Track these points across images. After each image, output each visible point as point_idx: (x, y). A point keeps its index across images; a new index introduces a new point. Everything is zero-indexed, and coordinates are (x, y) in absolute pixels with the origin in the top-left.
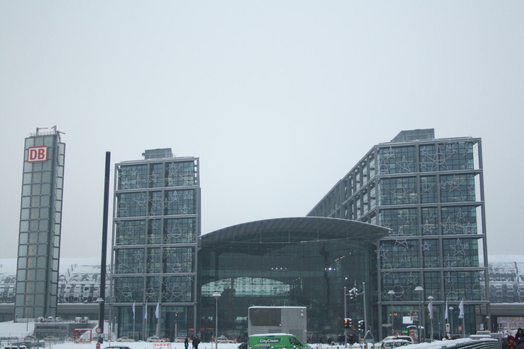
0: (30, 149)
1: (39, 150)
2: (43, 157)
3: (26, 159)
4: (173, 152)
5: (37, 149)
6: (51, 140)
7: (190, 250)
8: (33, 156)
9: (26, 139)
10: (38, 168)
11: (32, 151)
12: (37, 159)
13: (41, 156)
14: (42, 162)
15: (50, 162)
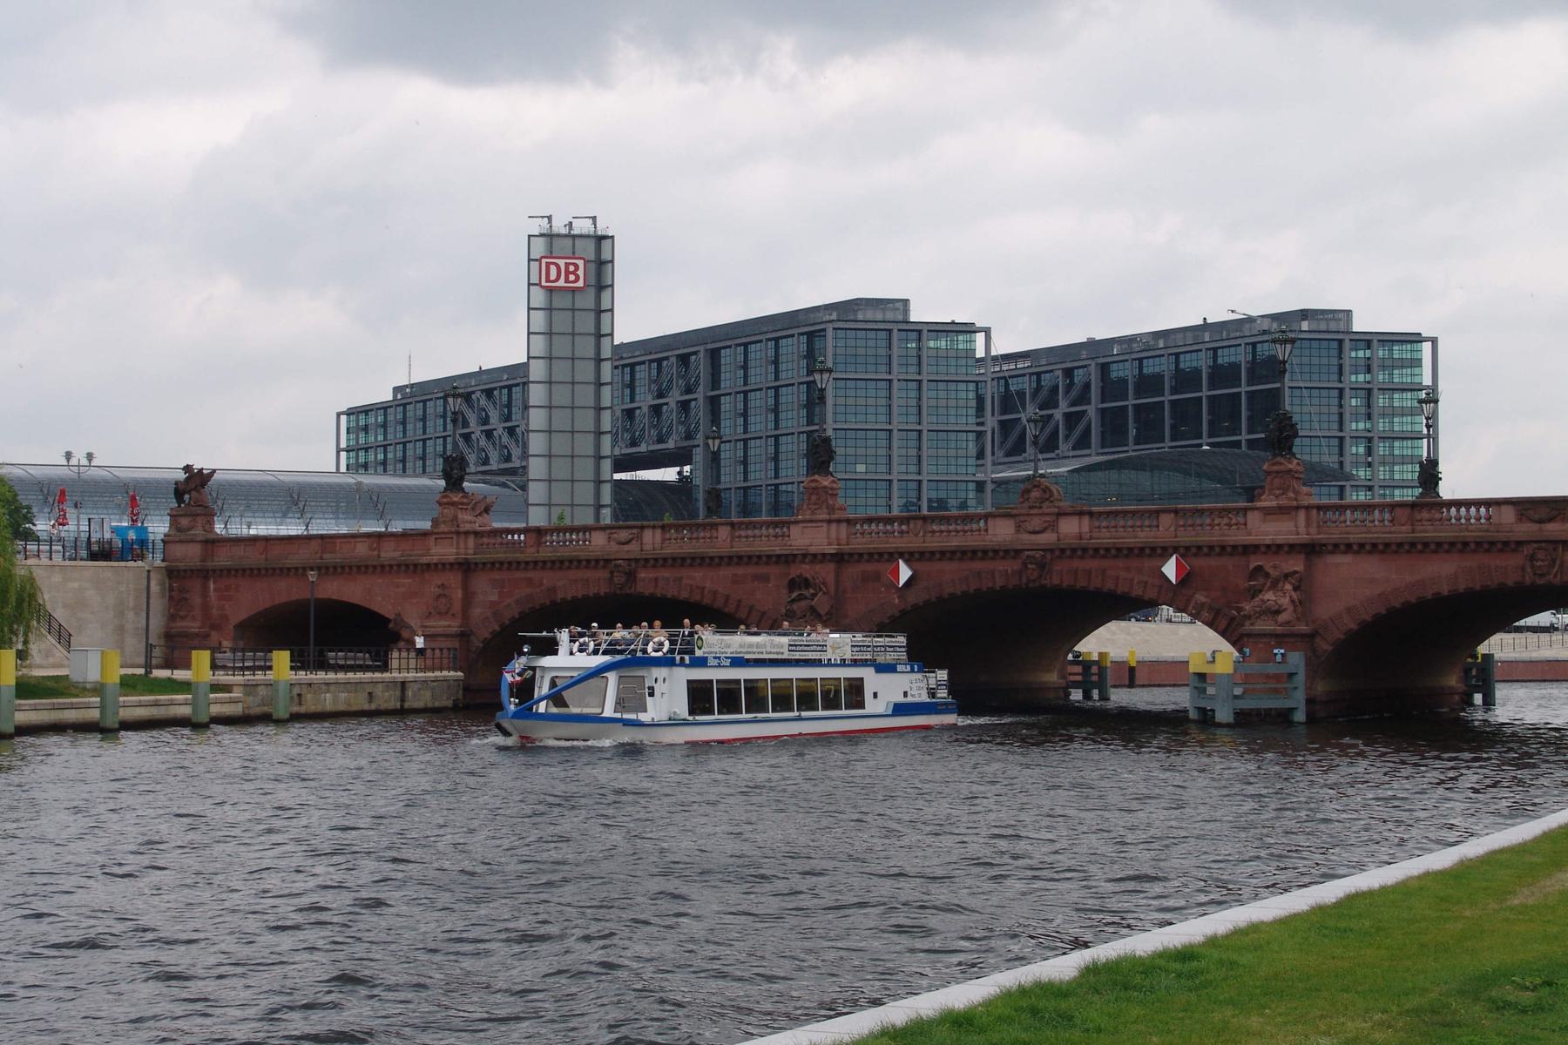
0: (544, 261)
1: (567, 265)
2: (577, 280)
3: (534, 280)
4: (913, 307)
5: (562, 263)
6: (591, 245)
7: (972, 486)
8: (553, 277)
9: (529, 236)
10: (561, 301)
11: (548, 265)
12: (561, 283)
13: (572, 277)
14: (574, 290)
15: (591, 292)
